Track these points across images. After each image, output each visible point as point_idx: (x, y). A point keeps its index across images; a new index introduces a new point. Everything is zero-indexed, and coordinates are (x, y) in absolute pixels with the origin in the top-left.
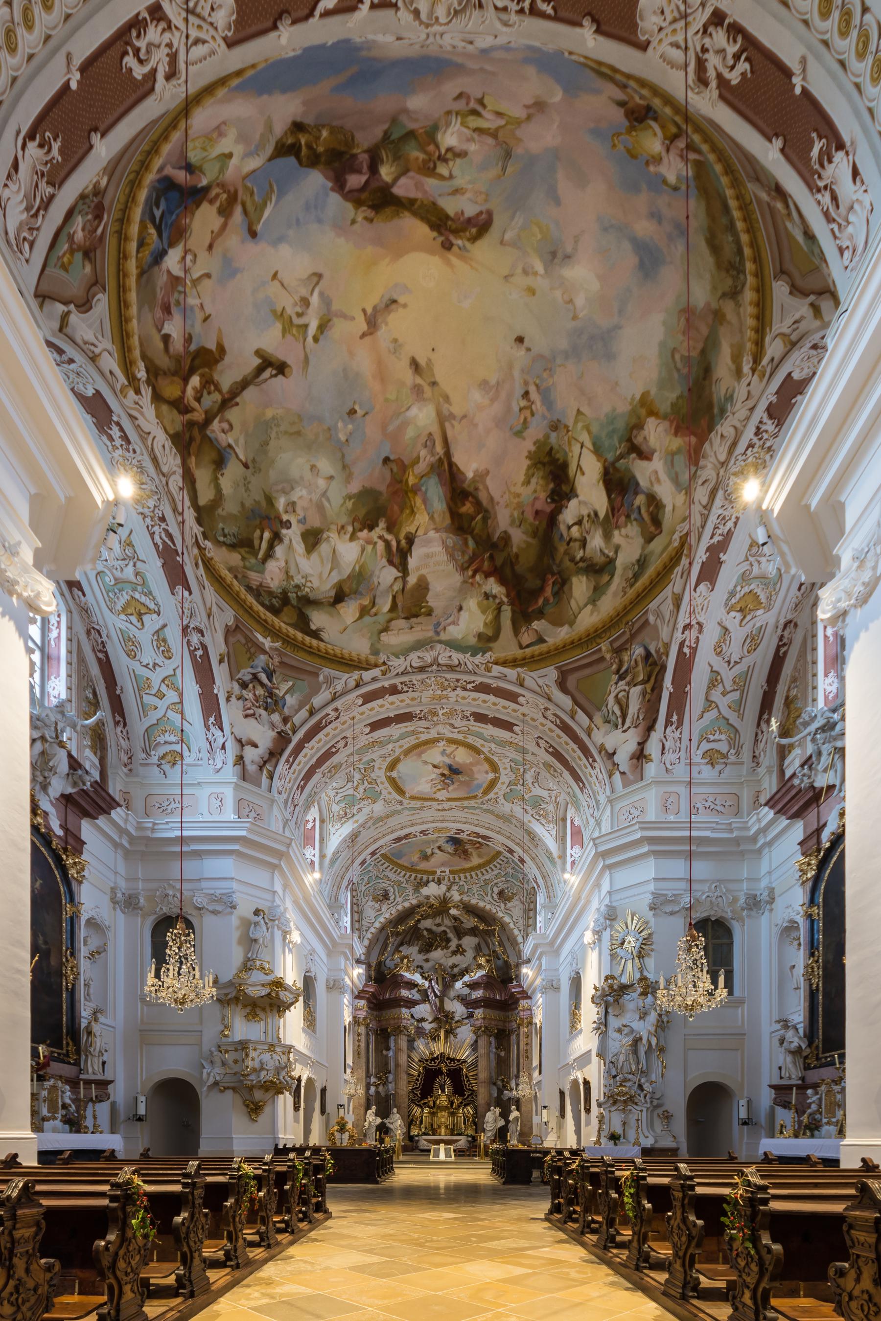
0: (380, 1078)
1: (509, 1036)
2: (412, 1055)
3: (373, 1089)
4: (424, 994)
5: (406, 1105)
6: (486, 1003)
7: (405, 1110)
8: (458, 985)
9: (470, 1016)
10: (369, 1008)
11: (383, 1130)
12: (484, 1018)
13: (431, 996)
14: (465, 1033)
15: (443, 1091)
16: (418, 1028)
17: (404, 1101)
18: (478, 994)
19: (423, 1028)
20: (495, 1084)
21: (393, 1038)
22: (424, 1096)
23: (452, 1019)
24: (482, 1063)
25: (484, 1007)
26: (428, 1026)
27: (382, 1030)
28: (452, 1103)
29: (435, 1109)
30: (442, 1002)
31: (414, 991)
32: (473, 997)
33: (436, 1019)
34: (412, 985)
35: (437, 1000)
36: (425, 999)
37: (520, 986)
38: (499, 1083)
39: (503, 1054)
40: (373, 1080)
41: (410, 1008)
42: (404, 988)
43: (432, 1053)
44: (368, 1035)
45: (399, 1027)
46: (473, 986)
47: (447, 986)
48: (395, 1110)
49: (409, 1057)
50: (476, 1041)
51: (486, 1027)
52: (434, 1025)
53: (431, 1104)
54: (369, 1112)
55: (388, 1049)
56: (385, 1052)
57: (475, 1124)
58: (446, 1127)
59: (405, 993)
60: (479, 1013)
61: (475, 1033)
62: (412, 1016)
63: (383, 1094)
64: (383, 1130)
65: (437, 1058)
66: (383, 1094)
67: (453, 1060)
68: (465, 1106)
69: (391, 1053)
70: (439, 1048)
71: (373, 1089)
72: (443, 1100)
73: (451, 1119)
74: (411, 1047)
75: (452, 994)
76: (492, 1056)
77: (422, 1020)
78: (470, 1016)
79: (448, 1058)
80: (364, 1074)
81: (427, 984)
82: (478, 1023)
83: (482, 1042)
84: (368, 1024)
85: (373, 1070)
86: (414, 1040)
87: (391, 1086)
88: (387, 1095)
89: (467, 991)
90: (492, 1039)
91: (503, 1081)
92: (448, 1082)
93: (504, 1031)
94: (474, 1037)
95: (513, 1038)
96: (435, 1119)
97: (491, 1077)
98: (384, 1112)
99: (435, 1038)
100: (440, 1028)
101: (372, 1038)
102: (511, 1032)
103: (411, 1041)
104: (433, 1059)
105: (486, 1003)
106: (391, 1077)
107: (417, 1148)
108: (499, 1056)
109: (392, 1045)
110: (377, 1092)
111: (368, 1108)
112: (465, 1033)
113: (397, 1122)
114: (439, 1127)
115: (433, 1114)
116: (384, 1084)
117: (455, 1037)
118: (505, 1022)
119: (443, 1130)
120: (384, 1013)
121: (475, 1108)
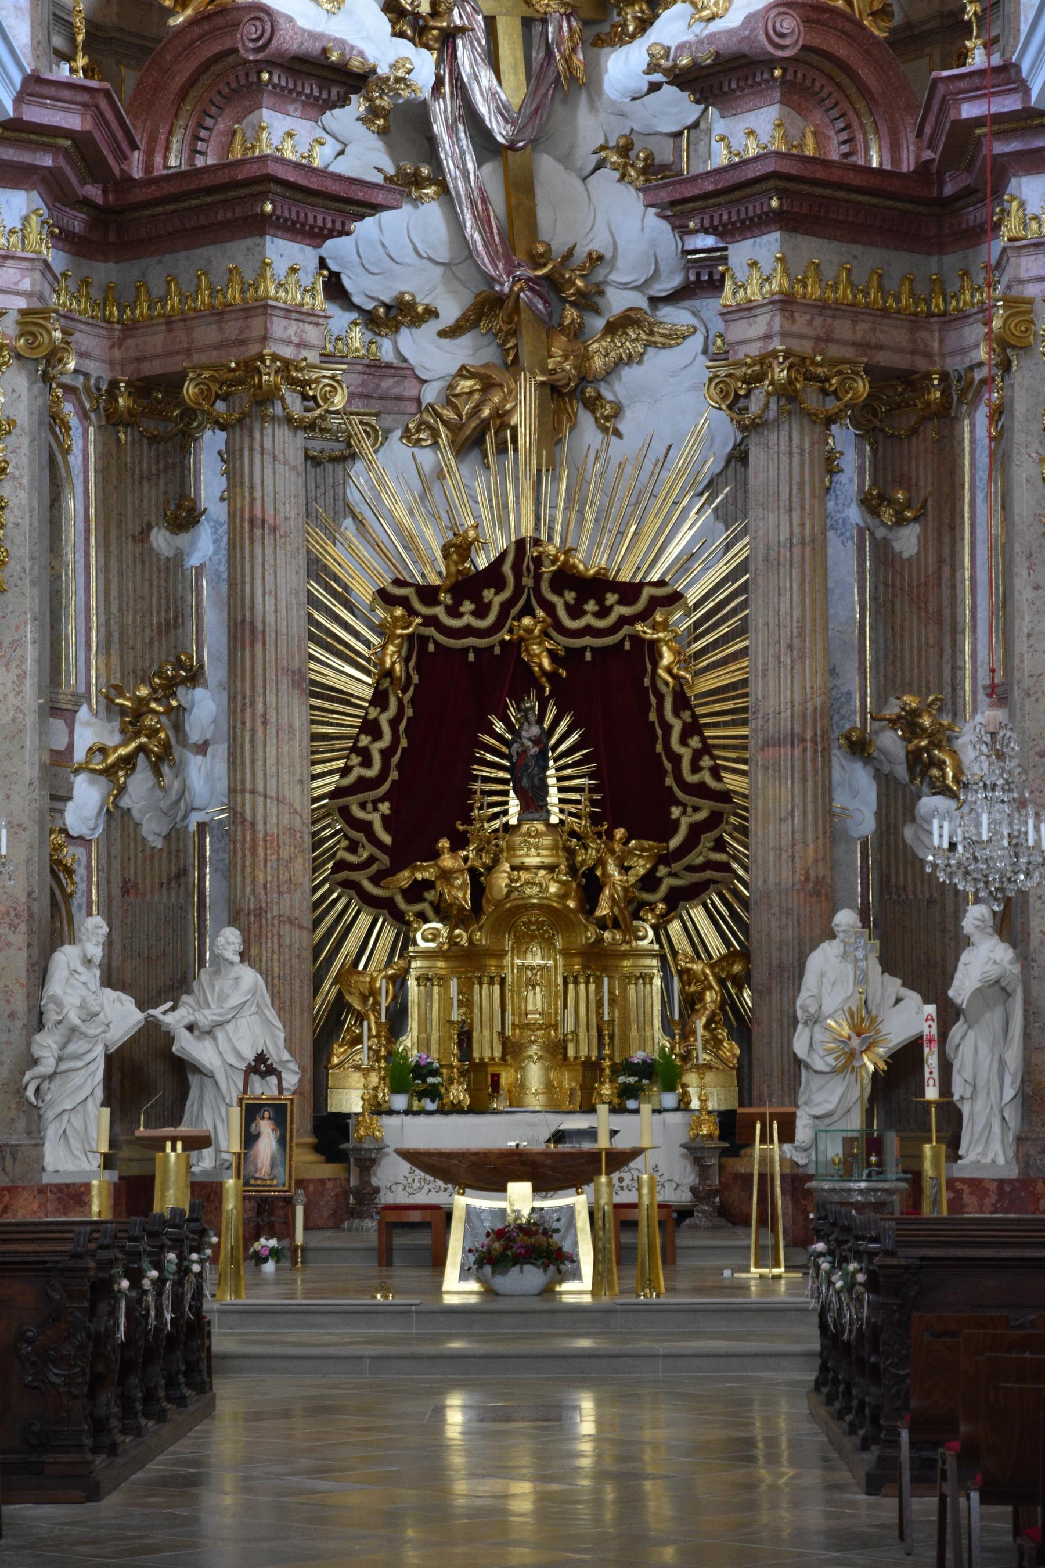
0: (133, 720)
1: (946, 415)
2: (335, 556)
3: (87, 798)
4: (406, 124)
5: (296, 904)
6: (798, 198)
7: (299, 940)
8: (624, 67)
9: (703, 280)
10: (63, 238)
11: (147, 1081)
12: (786, 303)
13: (455, 151)
14: (669, 402)
15: (534, 802)
16: (376, 367)
17: (290, 878)
18: (750, 133)
19: (402, 370)
20: (859, 748)
21: (211, 442)
22: (412, 842)
23: (589, 301)
24: (776, 609)
25: (788, 221)
26: (434, 357)
27: (142, 388)
28: (590, 887)
29: (488, 921)
30: (521, 189)
31: (347, 118)
32: (720, 157)
33: (487, 311)
34: (328, 78)
35: (491, 177)
36: (418, 174)
37: (1007, 77)
38: (891, 742)
39: (908, 541)
40: (90, 732)
41: (316, 236)
42: (284, 97)
43: (459, 548)
44: (55, 421)
45: (250, 367)
46: (715, 78)
47: (557, 84)
48: (229, 940)
49: (317, 569)
50: (739, 457)
51: (798, 363)
52: (464, 351)
53: (461, 895)
54: (66, 958)
55: (185, 517)
56: (161, 540)
57: (738, 1024)
58: (556, 1052)
59: (288, 135)
60: (758, 263)
61: (734, 403)
62: (335, 289)
63: (152, 830)
64: (147, 1081)
65: (493, 575)
66: (152, 830)
67: (596, 587)
68: (676, 899)
69: (204, 547)
70: (497, 511)
71: (87, 798)
72: (533, 866)
73: (583, 993)
74: (329, 509)
75: (590, 129)
76: (844, 560)
77: (397, 314)
78: (703, 280)
79: (567, 578)
80: (30, 699)
81: (423, 66)
82: (753, 336)
83: (774, 461)
84: (54, 356)
85: (86, 665)
86: (348, 456)
87: (203, 777)
88: (174, 835)
89: (676, 108)
90: (843, 437)
91: (909, 723)
92: (565, 736)
93: (911, 380)
94: (727, 435)
95: (975, 429)
96: (487, 996)
97: (832, 706)
98: (156, 966)
99: (478, 438)
100: (514, 366)
101: (83, 446)
102: (961, 391)
103: (331, 457)
104: (468, 586)
105: (798, 198)
106: (204, 707)
107: (367, 1194)
108: (883, 555)
109: (209, 483)
110: (116, 815)
111: (54, 928)
112: (669, 402)
113: (234, 1021)
114: (512, 1050)
115: (469, 963)
116: (162, 759)
117: (609, 423)
118: (916, 322)
119: (535, 1074)
120: (155, 270)
121: (738, 920)
